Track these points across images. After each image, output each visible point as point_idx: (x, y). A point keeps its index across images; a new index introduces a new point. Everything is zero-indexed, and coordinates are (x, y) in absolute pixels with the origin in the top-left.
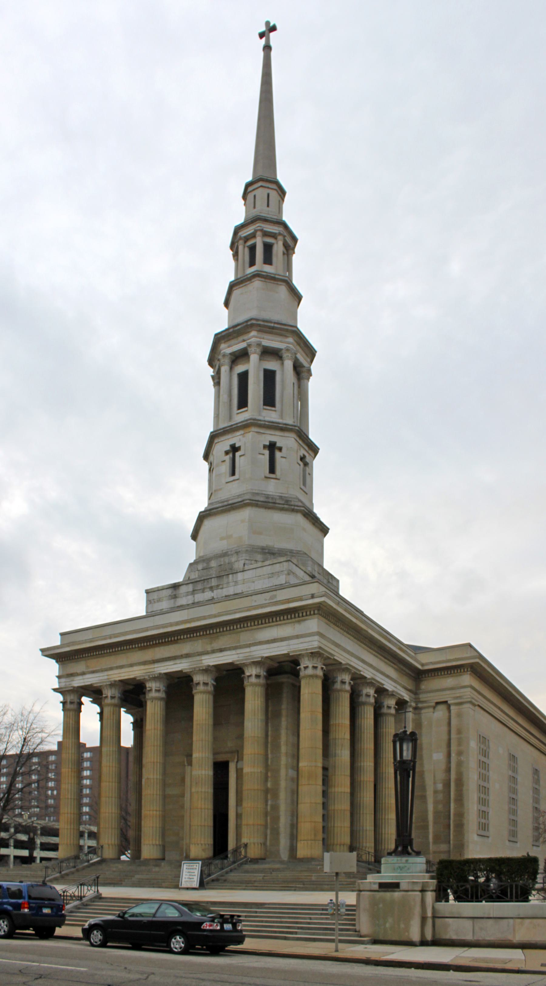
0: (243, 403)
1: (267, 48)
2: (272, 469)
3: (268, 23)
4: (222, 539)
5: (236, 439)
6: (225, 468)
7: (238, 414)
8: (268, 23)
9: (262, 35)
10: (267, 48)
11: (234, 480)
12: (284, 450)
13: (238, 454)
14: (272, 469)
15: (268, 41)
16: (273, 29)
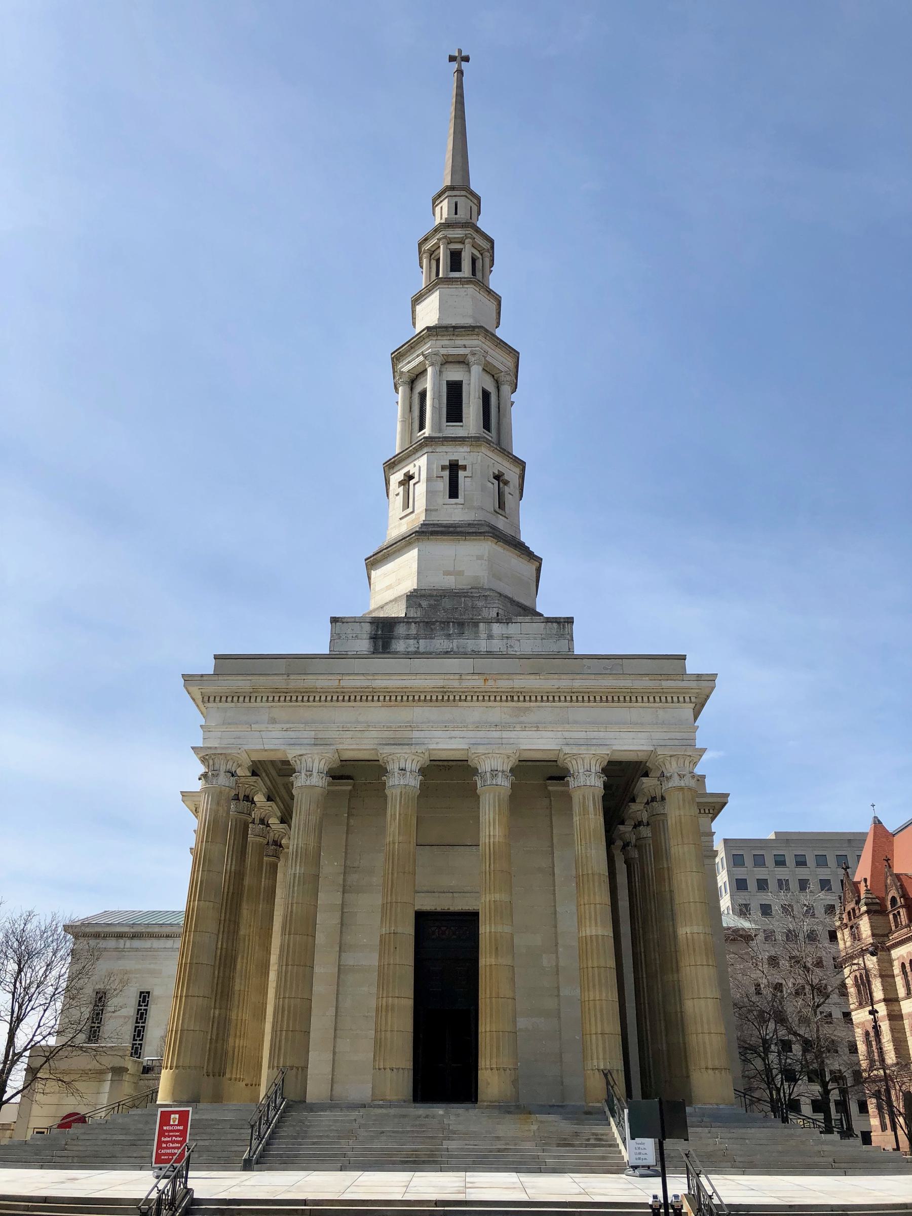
0: (454, 413)
1: (460, 72)
2: (501, 504)
3: (460, 51)
4: (447, 573)
5: (460, 454)
6: (443, 486)
7: (447, 426)
8: (460, 51)
9: (452, 59)
10: (460, 72)
11: (456, 504)
12: (511, 484)
13: (461, 474)
14: (501, 504)
15: (460, 65)
16: (466, 59)
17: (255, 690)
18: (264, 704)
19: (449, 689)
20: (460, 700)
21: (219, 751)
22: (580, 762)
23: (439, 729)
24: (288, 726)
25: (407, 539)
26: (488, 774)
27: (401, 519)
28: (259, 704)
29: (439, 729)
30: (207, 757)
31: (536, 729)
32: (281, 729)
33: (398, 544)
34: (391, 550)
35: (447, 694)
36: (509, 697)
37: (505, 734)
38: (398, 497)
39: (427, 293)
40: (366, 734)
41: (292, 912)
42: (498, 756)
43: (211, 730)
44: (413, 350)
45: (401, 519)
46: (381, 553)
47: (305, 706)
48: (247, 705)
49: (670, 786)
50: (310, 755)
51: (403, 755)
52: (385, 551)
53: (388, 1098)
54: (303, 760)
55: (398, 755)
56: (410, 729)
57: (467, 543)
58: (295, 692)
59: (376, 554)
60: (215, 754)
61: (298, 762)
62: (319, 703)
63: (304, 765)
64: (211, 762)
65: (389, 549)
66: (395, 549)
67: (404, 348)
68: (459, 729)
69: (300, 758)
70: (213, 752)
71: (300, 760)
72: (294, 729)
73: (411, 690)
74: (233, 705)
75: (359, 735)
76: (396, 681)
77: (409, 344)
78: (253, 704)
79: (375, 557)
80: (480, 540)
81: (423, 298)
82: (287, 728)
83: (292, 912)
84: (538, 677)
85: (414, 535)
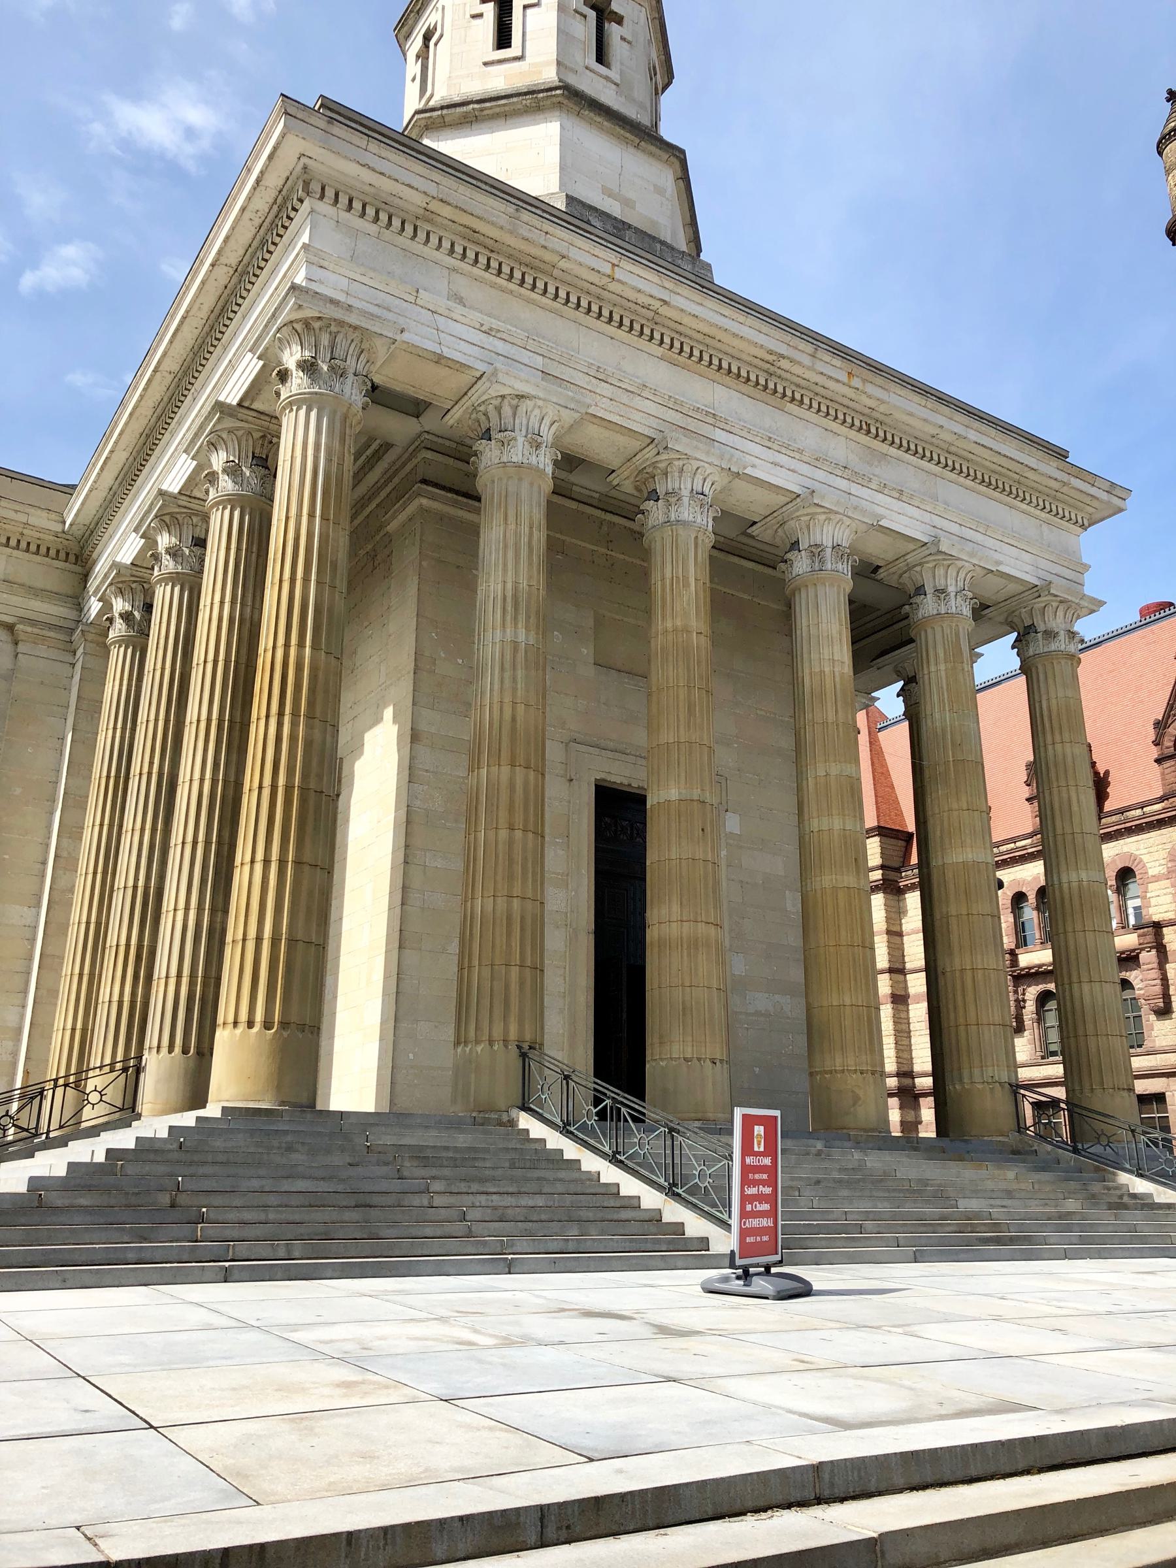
17: (428, 215)
18: (442, 256)
19: (779, 372)
20: (793, 399)
21: (353, 319)
22: (952, 572)
23: (757, 440)
24: (495, 324)
25: (541, 95)
26: (829, 551)
27: (485, 64)
28: (428, 251)
29: (757, 440)
30: (317, 325)
31: (897, 495)
32: (478, 326)
33: (515, 99)
34: (491, 108)
35: (774, 379)
36: (864, 423)
37: (855, 489)
38: (478, 21)
40: (638, 402)
41: (514, 719)
42: (848, 522)
43: (325, 264)
45: (485, 64)
46: (464, 109)
47: (520, 296)
48: (404, 241)
49: (1053, 648)
50: (540, 403)
51: (706, 465)
52: (476, 106)
53: (710, 1115)
54: (522, 410)
55: (695, 464)
56: (711, 421)
57: (639, 154)
58: (510, 257)
59: (449, 107)
60: (341, 323)
61: (507, 410)
62: (550, 302)
63: (521, 419)
64: (325, 340)
65: (488, 105)
66: (497, 110)
68: (788, 452)
69: (515, 402)
70: (338, 314)
71: (515, 408)
72: (504, 336)
73: (719, 345)
74: (373, 228)
75: (625, 398)
76: (711, 314)
78: (417, 247)
79: (445, 112)
80: (659, 159)
82: (491, 329)
83: (514, 719)
84: (923, 402)
85: (558, 92)
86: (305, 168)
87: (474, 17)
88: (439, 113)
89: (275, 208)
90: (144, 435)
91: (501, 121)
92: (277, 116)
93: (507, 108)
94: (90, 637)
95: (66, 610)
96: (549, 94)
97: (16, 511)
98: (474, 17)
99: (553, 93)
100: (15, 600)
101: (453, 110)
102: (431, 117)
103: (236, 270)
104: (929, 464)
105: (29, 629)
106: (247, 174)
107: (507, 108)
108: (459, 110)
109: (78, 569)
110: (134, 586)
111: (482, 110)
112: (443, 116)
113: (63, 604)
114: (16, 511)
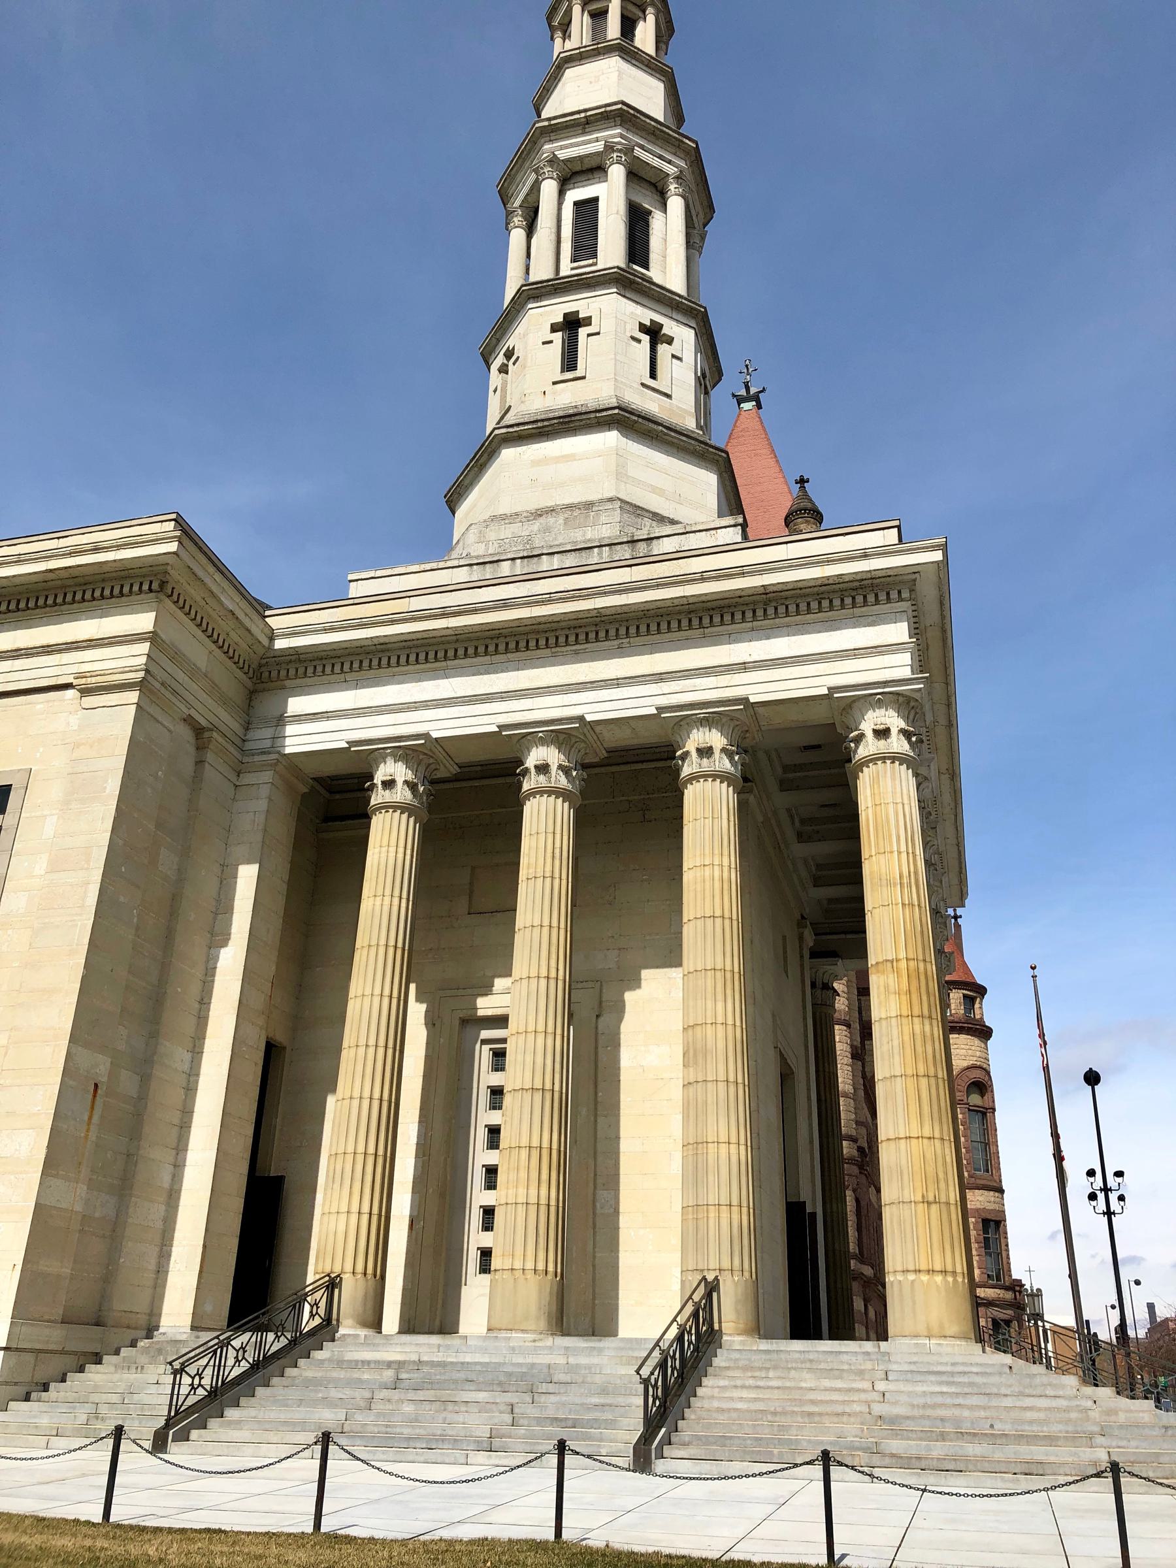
25: (711, 450)
34: (672, 437)
39: (642, 62)
44: (652, 138)
45: (643, 384)
46: (655, 427)
59: (644, 418)
66: (676, 441)
67: (648, 121)
77: (659, 126)
79: (640, 420)
81: (634, 62)
86: (915, 580)
87: (633, 338)
88: (636, 418)
89: (857, 584)
90: (498, 632)
91: (675, 451)
92: (937, 546)
93: (682, 443)
94: (280, 768)
95: (237, 725)
96: (717, 452)
97: (246, 615)
98: (633, 338)
99: (720, 453)
100: (210, 702)
101: (647, 423)
102: (628, 418)
103: (766, 594)
104: (185, 617)
105: (220, 740)
106: (861, 557)
107: (682, 443)
108: (651, 425)
109: (249, 684)
110: (421, 757)
111: (666, 434)
112: (636, 422)
113: (238, 718)
114: (246, 615)
